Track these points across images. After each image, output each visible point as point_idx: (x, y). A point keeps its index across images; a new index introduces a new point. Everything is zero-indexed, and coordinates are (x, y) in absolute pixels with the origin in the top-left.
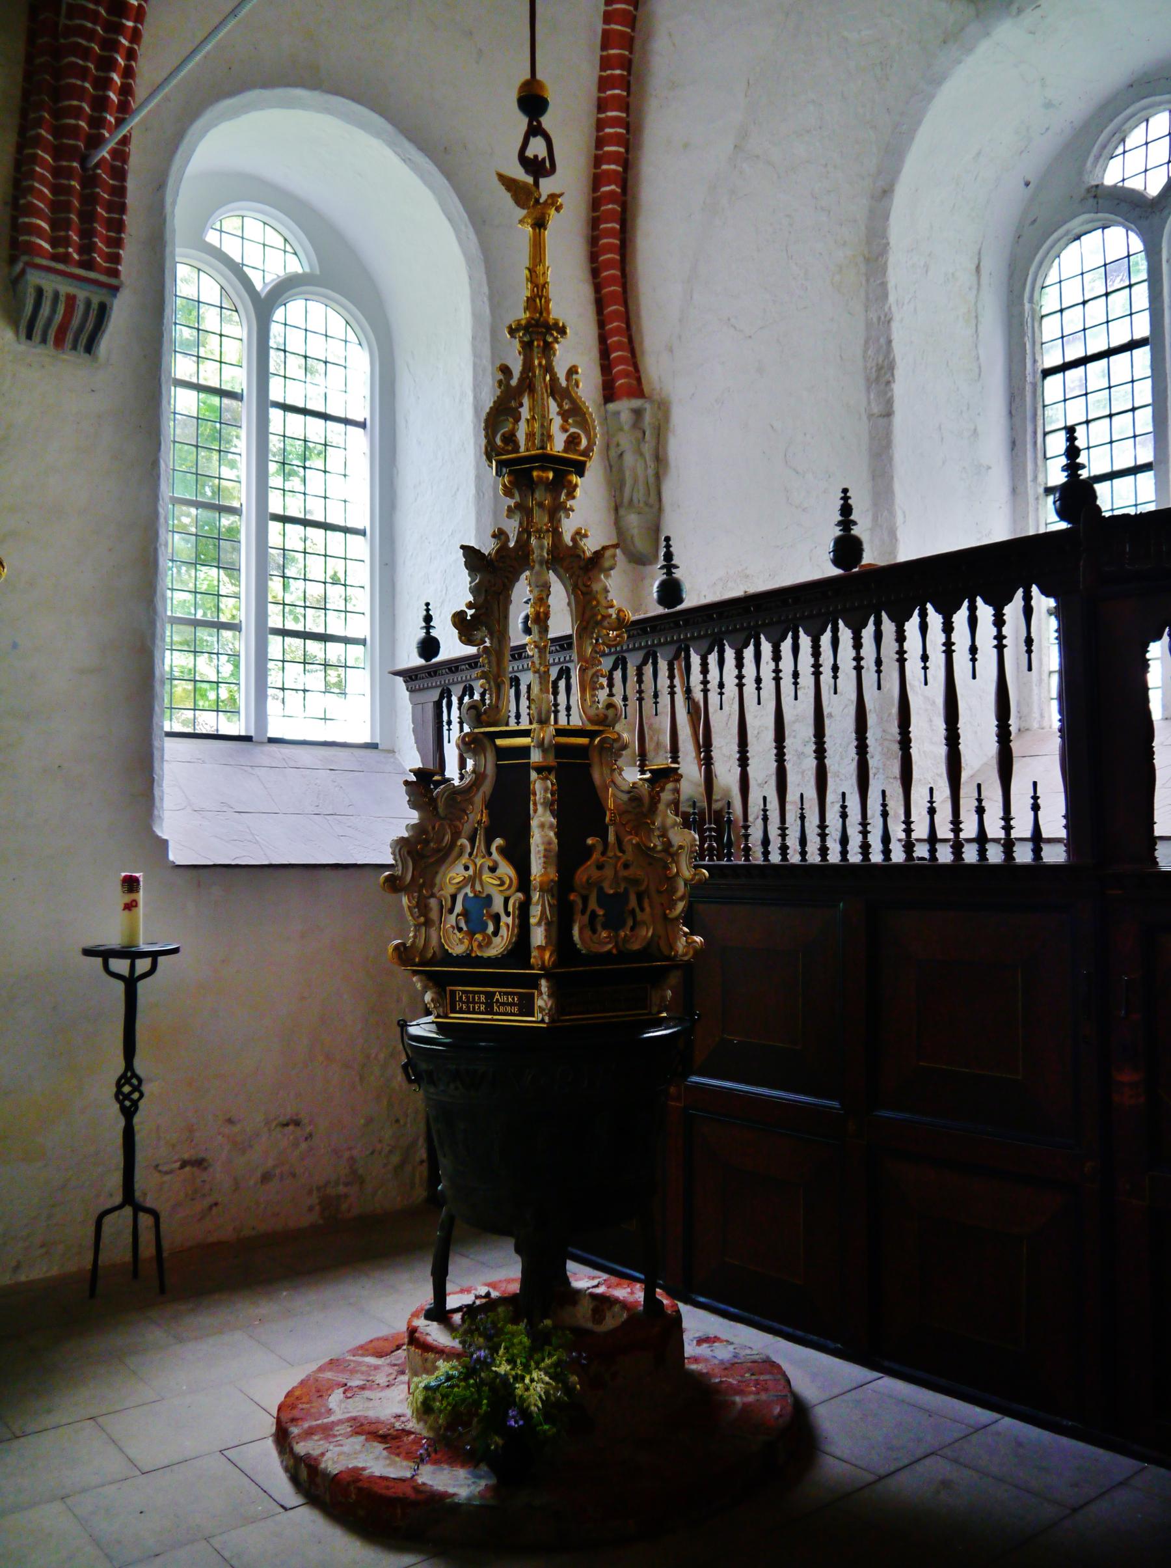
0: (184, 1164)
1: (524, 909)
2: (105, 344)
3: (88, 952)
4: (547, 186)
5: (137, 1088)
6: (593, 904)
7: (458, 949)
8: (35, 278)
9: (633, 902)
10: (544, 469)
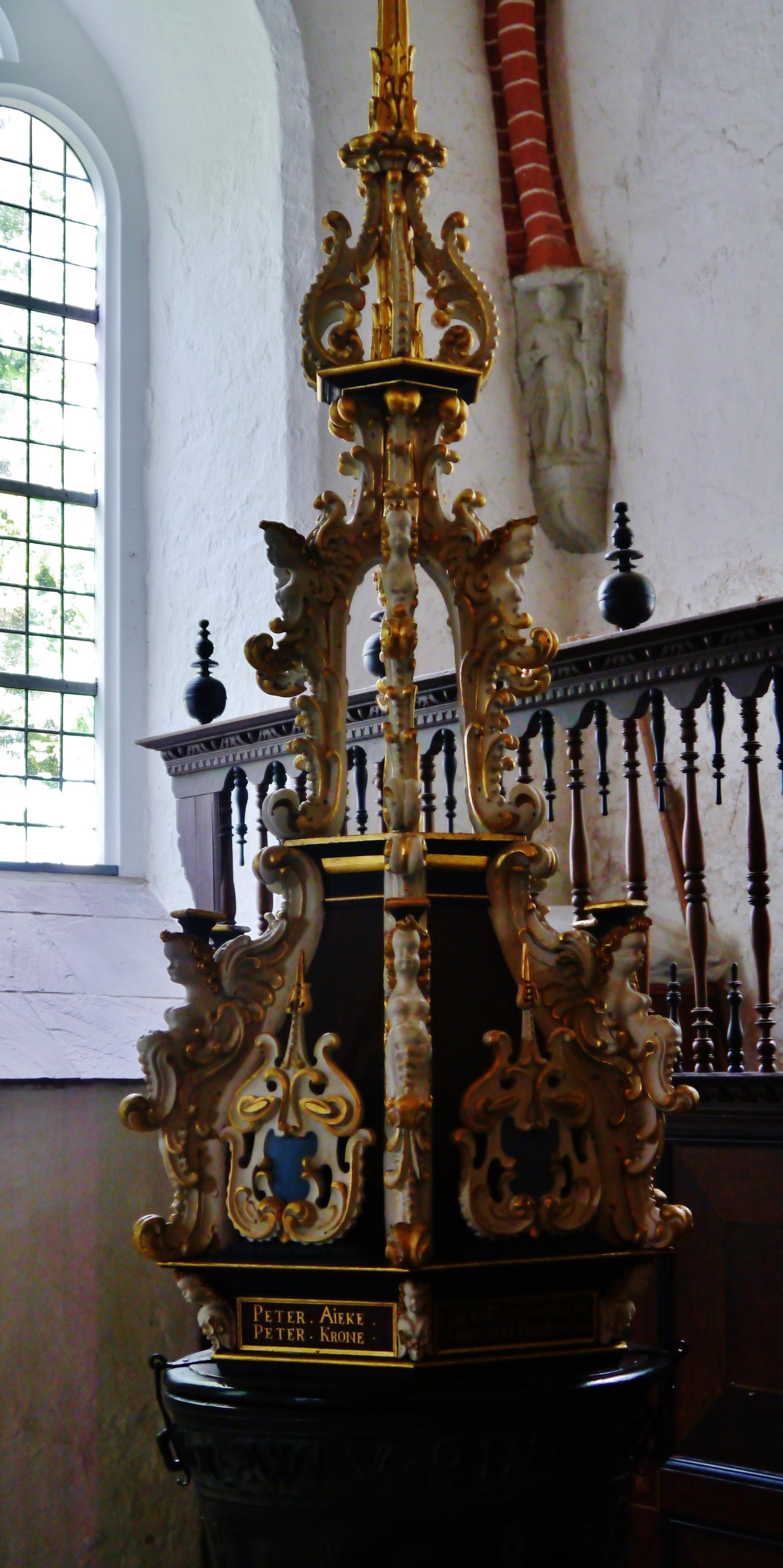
1: (373, 1158)
6: (495, 1150)
7: (256, 1230)
9: (566, 1147)
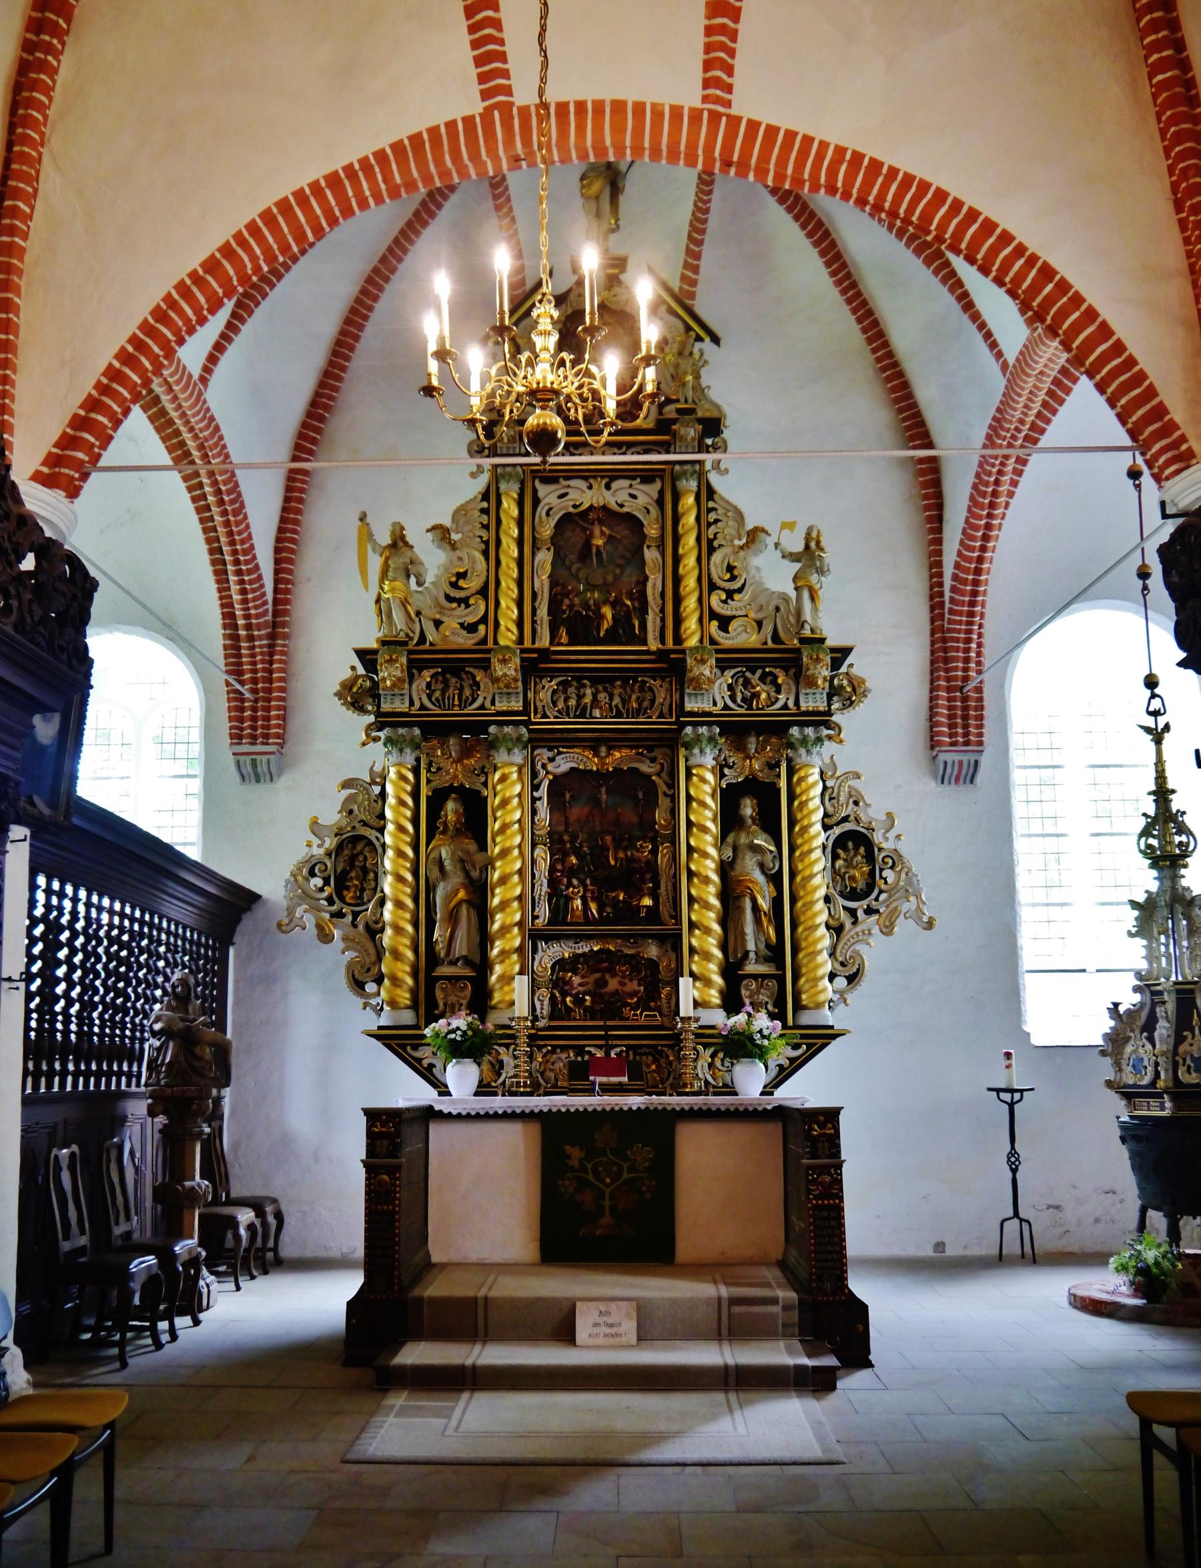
0: (1049, 1207)
1: (1157, 1064)
2: (979, 778)
3: (989, 1089)
5: (1017, 1159)
6: (1188, 1061)
7: (1131, 1082)
10: (1165, 861)
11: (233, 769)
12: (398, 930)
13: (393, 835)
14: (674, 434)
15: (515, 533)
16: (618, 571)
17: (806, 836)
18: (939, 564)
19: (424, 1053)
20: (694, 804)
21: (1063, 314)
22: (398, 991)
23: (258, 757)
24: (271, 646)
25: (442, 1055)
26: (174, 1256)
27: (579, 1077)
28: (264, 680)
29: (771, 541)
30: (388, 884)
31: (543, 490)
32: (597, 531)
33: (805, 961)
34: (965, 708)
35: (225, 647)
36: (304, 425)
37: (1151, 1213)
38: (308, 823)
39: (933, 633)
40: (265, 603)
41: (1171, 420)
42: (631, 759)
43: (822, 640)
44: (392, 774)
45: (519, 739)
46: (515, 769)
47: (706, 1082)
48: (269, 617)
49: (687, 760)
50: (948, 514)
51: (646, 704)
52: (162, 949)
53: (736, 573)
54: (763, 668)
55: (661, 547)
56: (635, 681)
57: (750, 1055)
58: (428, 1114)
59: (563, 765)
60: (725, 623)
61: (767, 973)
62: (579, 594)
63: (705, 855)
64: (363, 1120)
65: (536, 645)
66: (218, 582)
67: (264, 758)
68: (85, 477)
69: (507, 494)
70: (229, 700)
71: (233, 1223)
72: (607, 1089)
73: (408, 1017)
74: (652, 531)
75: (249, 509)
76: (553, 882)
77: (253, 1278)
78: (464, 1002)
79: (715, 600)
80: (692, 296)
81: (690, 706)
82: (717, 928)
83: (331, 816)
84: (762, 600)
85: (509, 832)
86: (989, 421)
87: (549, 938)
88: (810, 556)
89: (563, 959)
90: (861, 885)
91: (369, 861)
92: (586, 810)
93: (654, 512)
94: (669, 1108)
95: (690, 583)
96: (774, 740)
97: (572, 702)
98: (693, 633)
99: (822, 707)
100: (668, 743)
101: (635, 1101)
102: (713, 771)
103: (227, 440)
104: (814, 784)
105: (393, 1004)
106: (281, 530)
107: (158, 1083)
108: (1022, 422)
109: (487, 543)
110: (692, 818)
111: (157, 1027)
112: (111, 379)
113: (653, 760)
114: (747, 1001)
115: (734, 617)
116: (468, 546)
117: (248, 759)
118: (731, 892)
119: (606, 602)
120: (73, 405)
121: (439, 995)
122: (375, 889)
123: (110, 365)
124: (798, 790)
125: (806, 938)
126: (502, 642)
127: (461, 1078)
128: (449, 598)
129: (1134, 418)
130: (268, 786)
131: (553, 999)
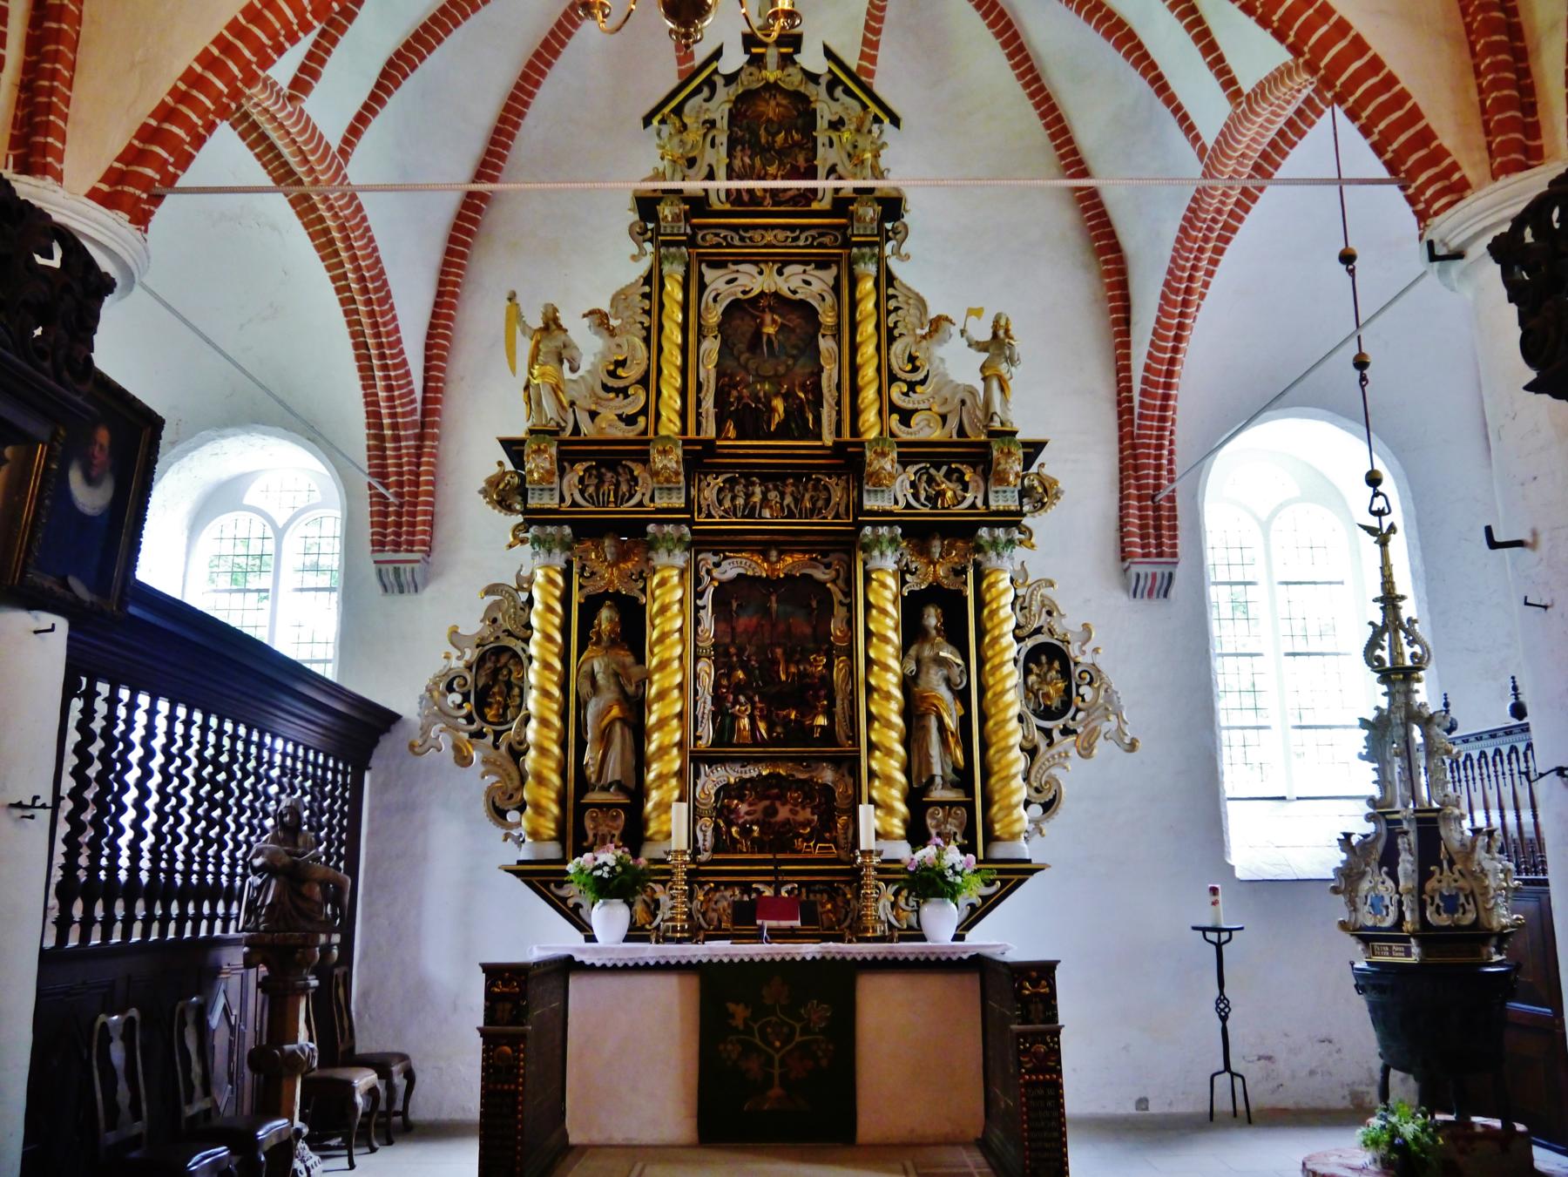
1: (1400, 903)
2: (1173, 592)
3: (1195, 928)
4: (1386, 521)
6: (1437, 900)
7: (1370, 923)
8: (1135, 569)
9: (1462, 900)
11: (374, 578)
12: (543, 751)
13: (540, 646)
14: (850, 216)
15: (680, 318)
16: (790, 362)
17: (997, 648)
18: (1128, 368)
19: (572, 892)
20: (874, 612)
21: (1309, 28)
22: (542, 821)
23: (402, 566)
24: (419, 448)
25: (590, 896)
26: (255, 1143)
27: (743, 922)
28: (411, 483)
29: (955, 330)
30: (532, 702)
31: (710, 275)
32: (768, 318)
33: (997, 787)
34: (1158, 518)
35: (369, 448)
36: (460, 216)
37: (1393, 1072)
38: (446, 632)
39: (1121, 440)
40: (413, 401)
41: (1440, 146)
42: (805, 566)
43: (1015, 433)
44: (540, 577)
45: (680, 539)
46: (676, 572)
47: (891, 926)
48: (417, 417)
49: (865, 564)
50: (1135, 317)
51: (820, 503)
52: (275, 773)
53: (918, 363)
54: (949, 464)
55: (837, 337)
56: (809, 479)
57: (941, 894)
58: (567, 966)
59: (729, 571)
60: (906, 417)
61: (955, 800)
62: (747, 385)
63: (886, 668)
64: (481, 978)
65: (702, 436)
66: (363, 378)
67: (408, 566)
68: (157, 199)
69: (670, 276)
70: (372, 504)
71: (348, 1087)
72: (778, 935)
73: (552, 850)
74: (827, 319)
75: (396, 299)
76: (717, 699)
77: (373, 1150)
78: (617, 833)
79: (896, 393)
80: (871, 74)
81: (869, 503)
82: (899, 749)
83: (473, 625)
84: (946, 393)
85: (668, 641)
86: (1183, 211)
87: (713, 760)
88: (998, 344)
89: (728, 784)
90: (1055, 703)
91: (515, 675)
92: (755, 620)
93: (830, 299)
94: (849, 958)
95: (868, 373)
96: (960, 544)
97: (740, 501)
98: (871, 427)
99: (1014, 506)
100: (844, 546)
101: (810, 950)
102: (894, 575)
103: (371, 222)
104: (1006, 590)
105: (535, 834)
106: (432, 326)
107: (256, 929)
108: (1219, 211)
109: (648, 329)
110: (872, 627)
111: (257, 862)
112: (191, 86)
113: (828, 566)
114: (933, 832)
115: (917, 410)
116: (628, 332)
117: (390, 567)
118: (915, 710)
119: (777, 394)
120: (143, 112)
121: (589, 825)
122: (520, 707)
123: (190, 69)
124: (988, 597)
125: (999, 761)
126: (663, 432)
127: (608, 919)
128: (606, 388)
129: (1395, 145)
130: (414, 597)
131: (716, 829)
